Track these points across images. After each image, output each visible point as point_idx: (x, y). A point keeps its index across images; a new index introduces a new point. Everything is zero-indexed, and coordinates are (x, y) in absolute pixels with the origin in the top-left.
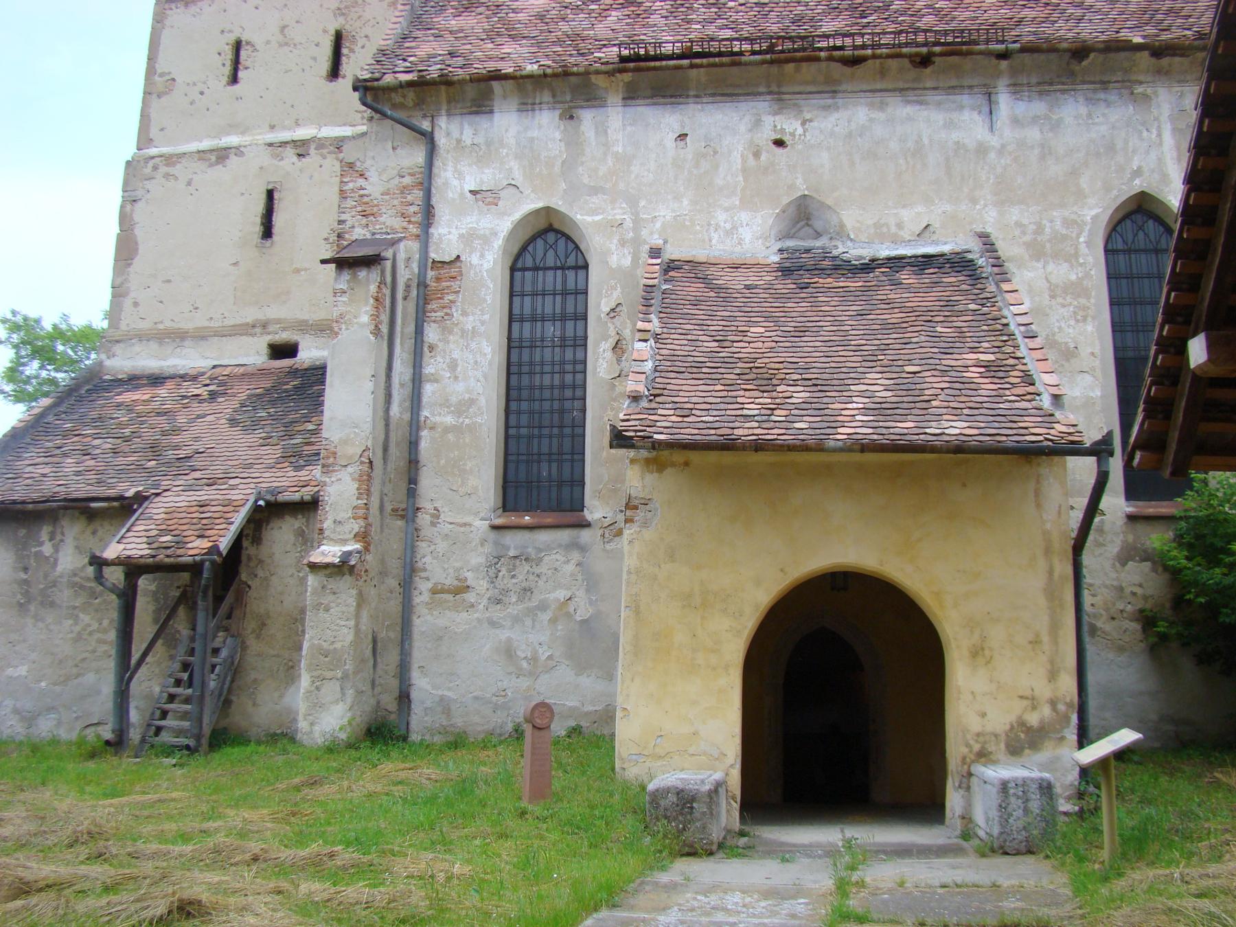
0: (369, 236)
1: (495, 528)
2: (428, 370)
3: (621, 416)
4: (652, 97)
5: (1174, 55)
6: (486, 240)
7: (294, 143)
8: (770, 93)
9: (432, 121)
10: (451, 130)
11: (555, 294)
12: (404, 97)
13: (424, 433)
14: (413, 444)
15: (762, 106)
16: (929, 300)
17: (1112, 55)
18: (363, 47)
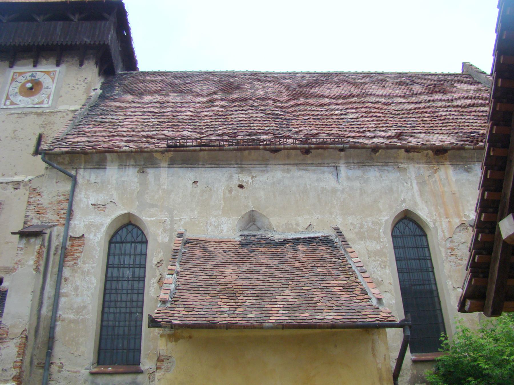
0: (40, 223)
1: (92, 374)
2: (63, 290)
3: (156, 311)
4: (182, 164)
5: (414, 152)
6: (98, 228)
7: (13, 183)
8: (237, 164)
9: (76, 171)
10: (85, 176)
11: (130, 255)
12: (64, 159)
13: (59, 323)
14: (52, 329)
15: (233, 170)
16: (313, 257)
17: (389, 151)
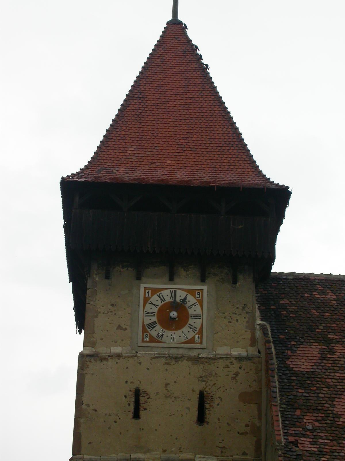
18: (218, 405)
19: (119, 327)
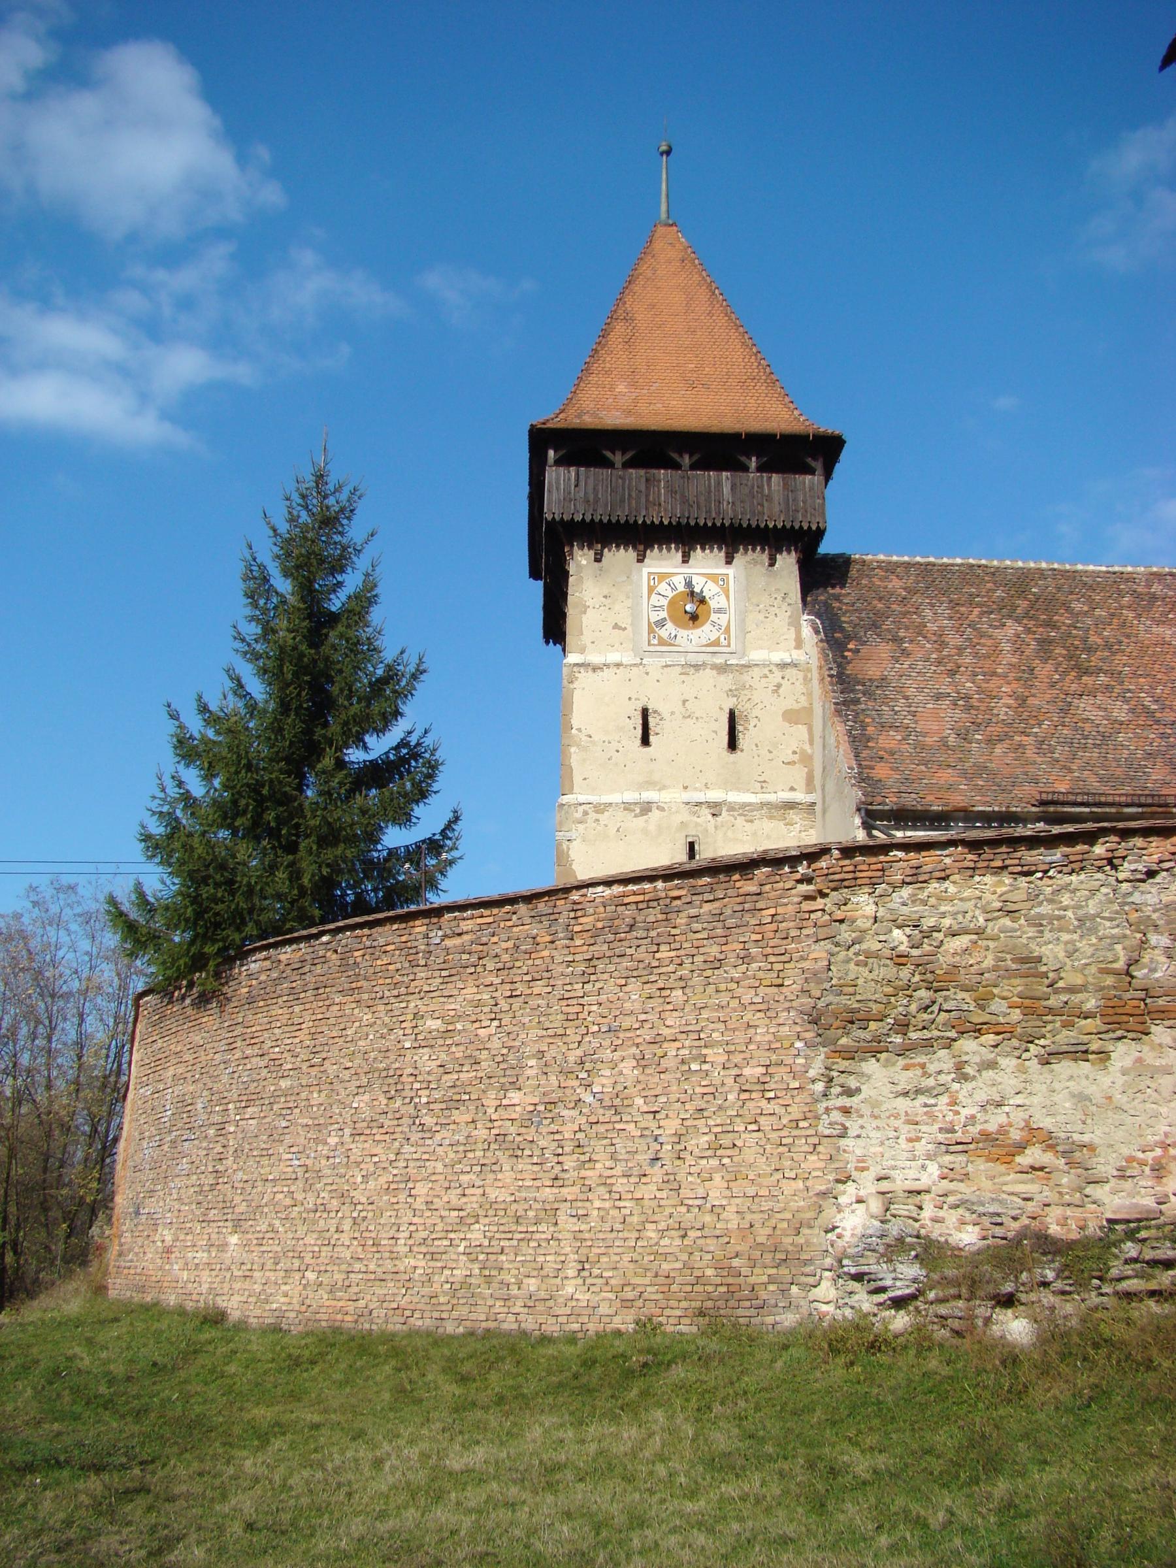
7: (710, 805)
19: (616, 626)
